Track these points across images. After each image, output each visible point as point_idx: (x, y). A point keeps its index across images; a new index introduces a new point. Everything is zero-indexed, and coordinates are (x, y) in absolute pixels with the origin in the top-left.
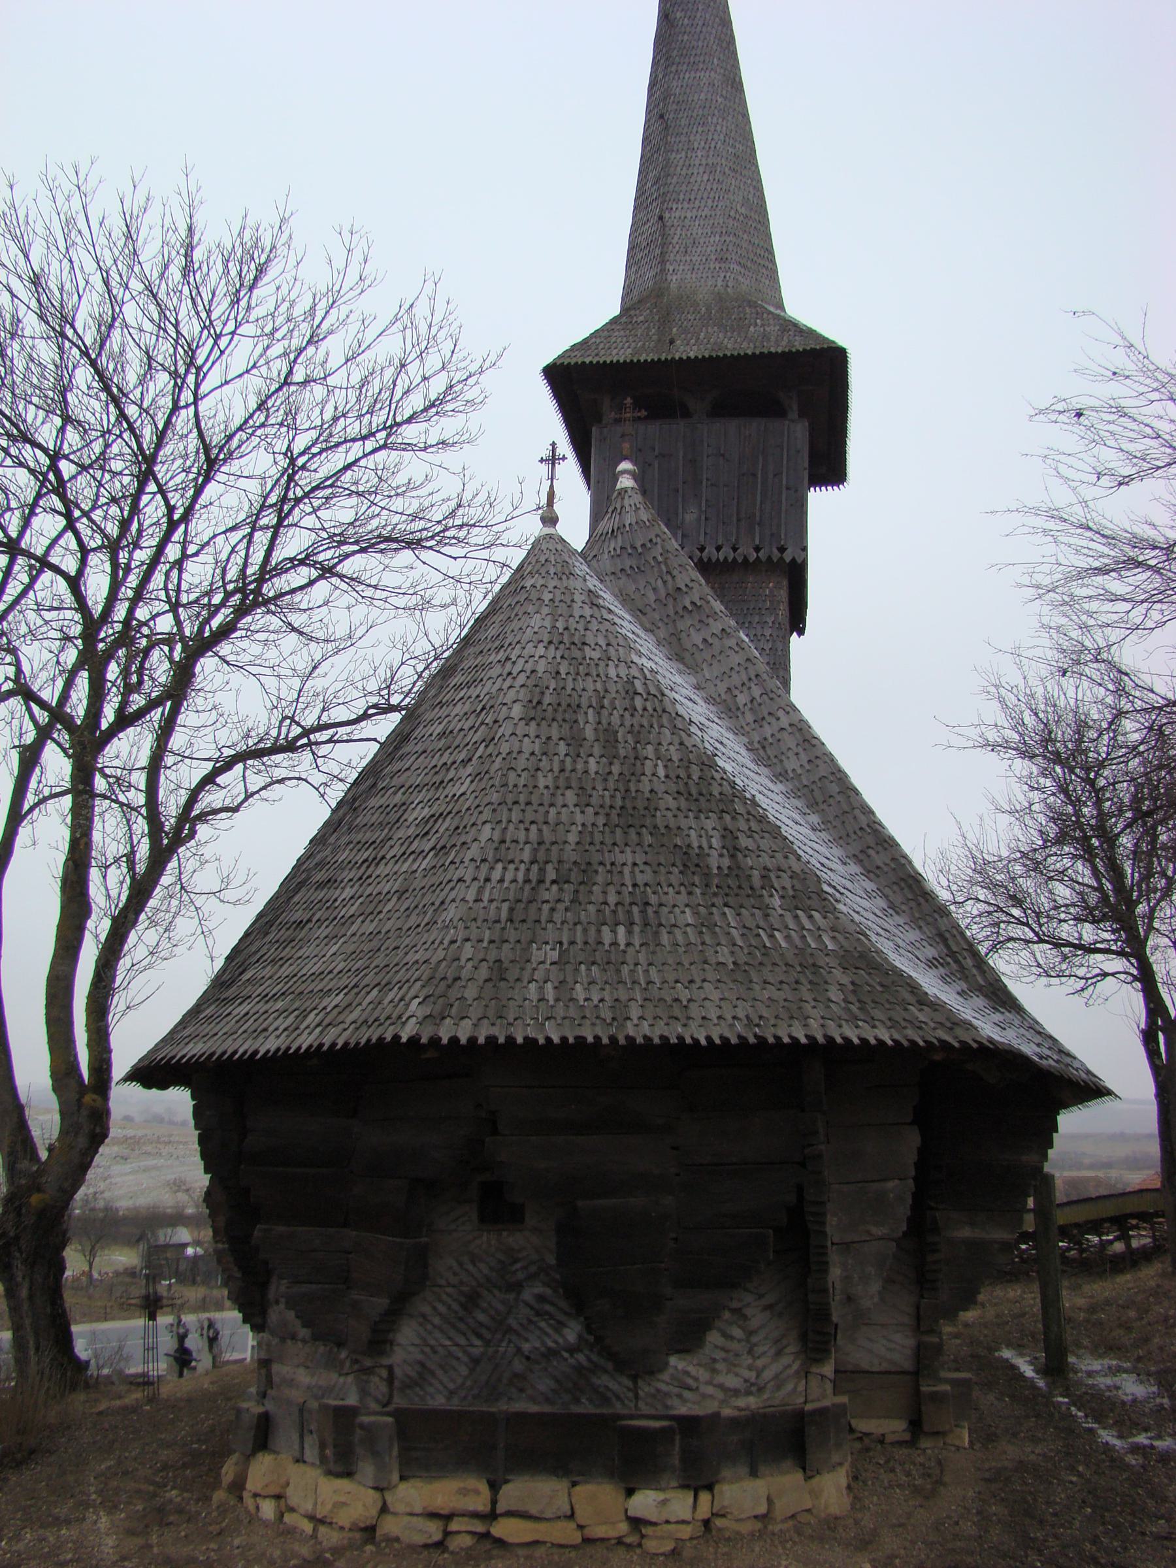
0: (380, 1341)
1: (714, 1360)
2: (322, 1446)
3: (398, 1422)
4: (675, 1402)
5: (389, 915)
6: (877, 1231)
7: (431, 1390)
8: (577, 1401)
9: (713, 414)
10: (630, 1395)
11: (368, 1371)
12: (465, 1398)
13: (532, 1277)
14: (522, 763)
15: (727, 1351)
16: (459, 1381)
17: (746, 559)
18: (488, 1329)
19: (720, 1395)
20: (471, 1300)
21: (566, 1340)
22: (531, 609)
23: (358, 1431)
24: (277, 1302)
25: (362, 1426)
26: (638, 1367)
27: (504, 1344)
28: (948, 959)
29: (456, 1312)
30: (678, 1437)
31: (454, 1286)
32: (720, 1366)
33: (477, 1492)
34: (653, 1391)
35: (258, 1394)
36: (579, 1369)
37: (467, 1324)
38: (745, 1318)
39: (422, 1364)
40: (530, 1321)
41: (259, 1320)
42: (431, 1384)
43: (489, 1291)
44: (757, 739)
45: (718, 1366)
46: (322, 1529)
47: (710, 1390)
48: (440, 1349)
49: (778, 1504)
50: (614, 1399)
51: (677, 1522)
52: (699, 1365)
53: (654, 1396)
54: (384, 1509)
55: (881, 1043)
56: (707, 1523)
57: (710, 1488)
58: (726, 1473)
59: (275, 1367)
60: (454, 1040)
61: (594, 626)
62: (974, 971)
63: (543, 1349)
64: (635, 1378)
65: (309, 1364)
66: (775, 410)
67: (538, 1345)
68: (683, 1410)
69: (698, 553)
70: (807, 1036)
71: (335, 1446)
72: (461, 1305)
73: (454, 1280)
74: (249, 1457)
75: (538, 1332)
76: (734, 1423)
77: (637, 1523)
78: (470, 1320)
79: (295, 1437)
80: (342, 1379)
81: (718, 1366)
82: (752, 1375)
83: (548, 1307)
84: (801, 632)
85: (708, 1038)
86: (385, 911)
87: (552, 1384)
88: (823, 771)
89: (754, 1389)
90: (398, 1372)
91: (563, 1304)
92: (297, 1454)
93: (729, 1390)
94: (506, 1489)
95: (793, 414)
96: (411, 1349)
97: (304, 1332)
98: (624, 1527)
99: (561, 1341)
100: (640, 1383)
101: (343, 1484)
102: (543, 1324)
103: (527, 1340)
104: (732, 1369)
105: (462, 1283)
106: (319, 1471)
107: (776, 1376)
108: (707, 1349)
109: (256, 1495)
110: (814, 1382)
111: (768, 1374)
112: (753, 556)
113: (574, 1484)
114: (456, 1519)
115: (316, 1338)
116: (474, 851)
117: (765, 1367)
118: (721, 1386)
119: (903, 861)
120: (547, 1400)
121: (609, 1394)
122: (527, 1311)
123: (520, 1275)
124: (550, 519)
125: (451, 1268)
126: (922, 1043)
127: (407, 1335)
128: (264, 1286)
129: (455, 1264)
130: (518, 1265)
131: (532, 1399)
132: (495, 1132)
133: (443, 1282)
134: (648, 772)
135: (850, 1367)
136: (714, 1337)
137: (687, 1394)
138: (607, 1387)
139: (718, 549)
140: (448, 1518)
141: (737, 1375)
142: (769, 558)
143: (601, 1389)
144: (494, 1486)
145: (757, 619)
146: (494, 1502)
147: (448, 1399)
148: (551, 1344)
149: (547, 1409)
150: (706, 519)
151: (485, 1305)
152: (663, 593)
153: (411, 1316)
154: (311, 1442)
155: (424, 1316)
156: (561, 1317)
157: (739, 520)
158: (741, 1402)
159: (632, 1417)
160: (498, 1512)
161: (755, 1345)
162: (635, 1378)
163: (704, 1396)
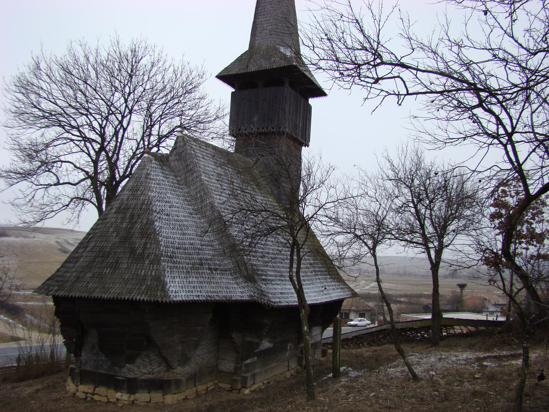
19: (141, 374)
38: (150, 357)
44: (200, 206)
47: (137, 372)
49: (152, 400)
56: (133, 402)
68: (129, 376)
76: (144, 380)
90: (82, 361)
94: (97, 389)
104: (142, 369)
107: (158, 371)
111: (155, 370)
118: (141, 372)
127: (83, 353)
139: (263, 129)
140: (87, 393)
152: (184, 166)
158: (147, 376)
162: (120, 368)
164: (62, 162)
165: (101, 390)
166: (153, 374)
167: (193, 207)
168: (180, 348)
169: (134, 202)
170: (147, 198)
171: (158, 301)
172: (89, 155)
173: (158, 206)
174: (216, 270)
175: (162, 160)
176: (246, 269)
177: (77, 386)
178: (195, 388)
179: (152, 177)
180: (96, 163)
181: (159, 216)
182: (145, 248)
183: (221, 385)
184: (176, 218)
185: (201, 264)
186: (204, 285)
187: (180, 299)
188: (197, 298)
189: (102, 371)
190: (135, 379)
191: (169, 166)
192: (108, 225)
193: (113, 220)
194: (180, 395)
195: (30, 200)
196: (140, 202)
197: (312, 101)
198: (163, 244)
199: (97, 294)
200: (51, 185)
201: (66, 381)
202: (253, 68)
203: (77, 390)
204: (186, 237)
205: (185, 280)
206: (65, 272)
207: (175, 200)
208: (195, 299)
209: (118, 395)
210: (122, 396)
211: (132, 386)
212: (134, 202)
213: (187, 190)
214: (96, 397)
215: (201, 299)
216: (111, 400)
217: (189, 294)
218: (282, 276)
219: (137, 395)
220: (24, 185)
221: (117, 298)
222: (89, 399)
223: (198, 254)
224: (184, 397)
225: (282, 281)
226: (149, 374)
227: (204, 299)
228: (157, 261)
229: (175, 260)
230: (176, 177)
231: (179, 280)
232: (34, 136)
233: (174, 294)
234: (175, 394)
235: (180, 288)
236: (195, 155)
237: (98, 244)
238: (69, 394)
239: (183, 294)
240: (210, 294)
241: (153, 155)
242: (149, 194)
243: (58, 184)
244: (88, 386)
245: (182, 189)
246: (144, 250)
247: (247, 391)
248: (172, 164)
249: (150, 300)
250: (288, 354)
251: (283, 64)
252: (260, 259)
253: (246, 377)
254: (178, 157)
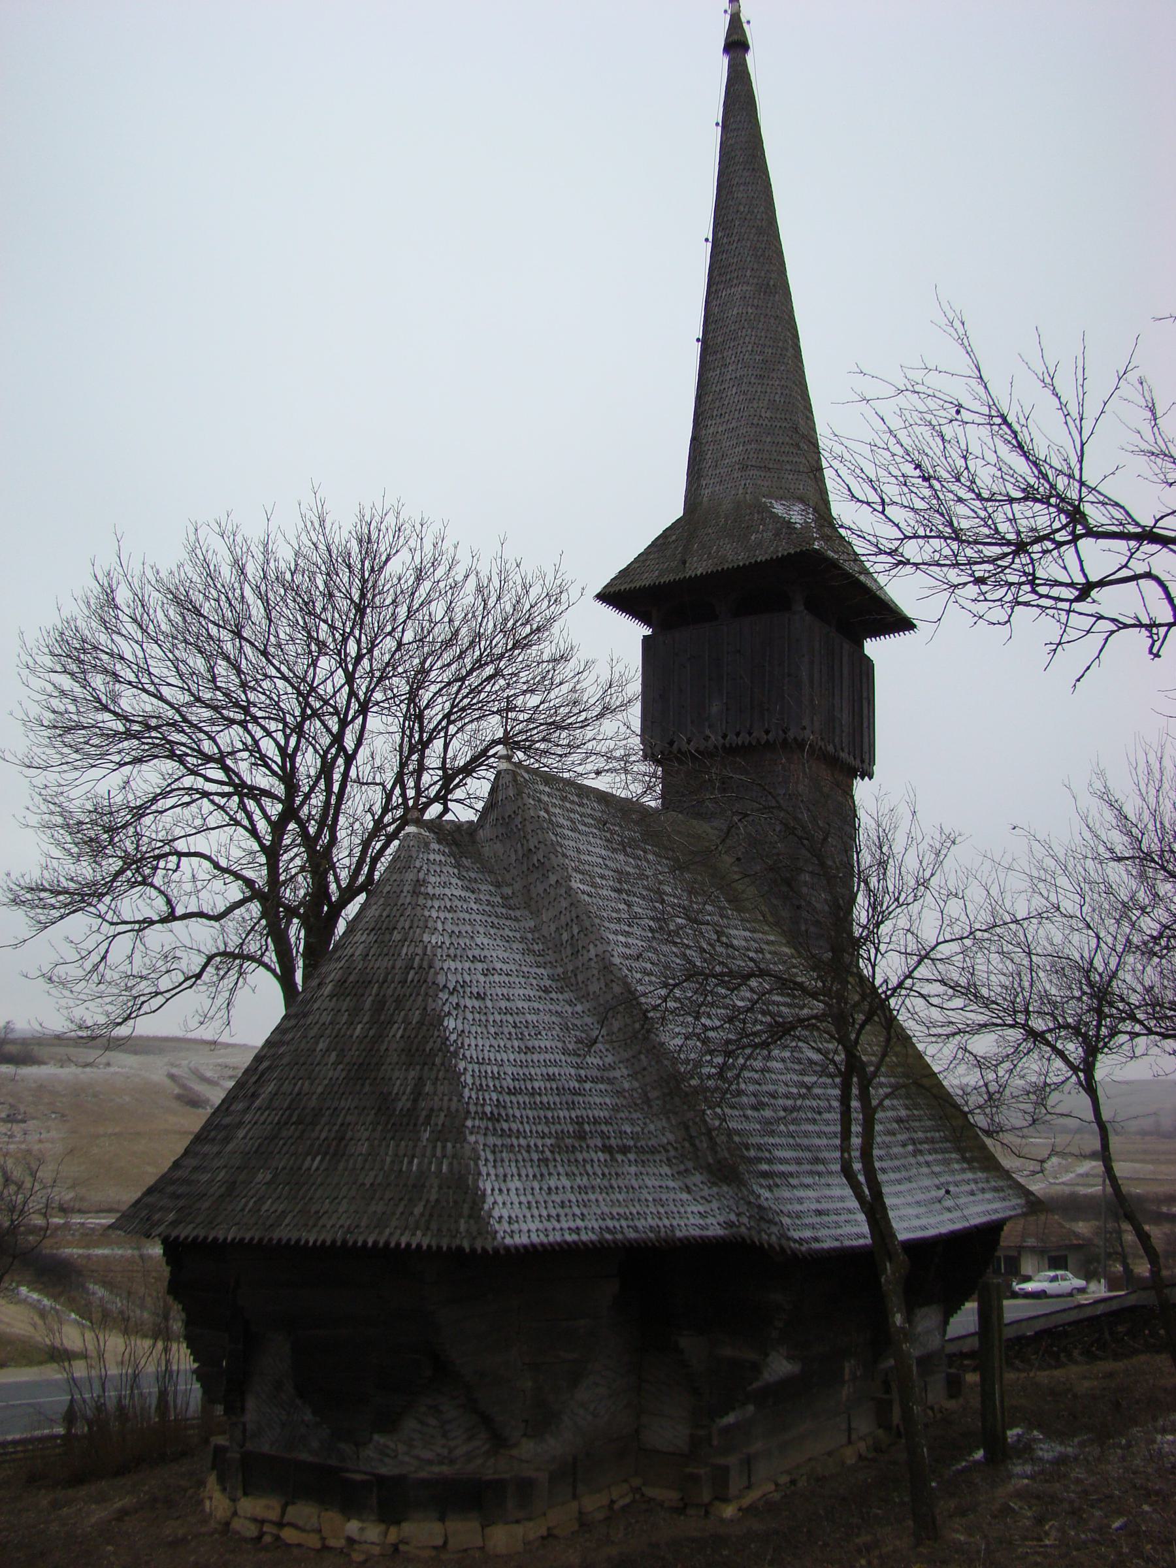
17: (758, 741)
44: (571, 968)
47: (407, 1459)
54: (235, 1514)
56: (396, 1548)
68: (383, 1471)
82: (445, 1452)
94: (291, 1510)
118: (417, 1458)
127: (251, 1403)
137: (386, 1460)
139: (738, 734)
140: (262, 1522)
152: (520, 853)
158: (436, 1469)
164: (180, 855)
165: (304, 1512)
166: (452, 1462)
167: (550, 971)
168: (530, 1384)
169: (385, 963)
170: (419, 951)
171: (460, 1249)
172: (254, 832)
173: (451, 971)
174: (625, 1150)
175: (458, 839)
176: (713, 1146)
177: (234, 1500)
178: (574, 1505)
179: (430, 890)
180: (272, 853)
181: (454, 1000)
182: (417, 1094)
183: (650, 1492)
184: (503, 1004)
185: (581, 1136)
186: (592, 1197)
187: (525, 1240)
188: (575, 1237)
189: (305, 1456)
190: (400, 1479)
191: (478, 857)
192: (312, 1033)
193: (326, 1018)
194: (531, 1524)
195: (96, 967)
196: (399, 964)
197: (873, 648)
198: (470, 1081)
199: (283, 1233)
200: (152, 923)
201: (202, 1483)
202: (699, 567)
203: (235, 1514)
204: (535, 1057)
205: (536, 1185)
206: (195, 1169)
207: (497, 953)
208: (568, 1238)
209: (353, 1527)
210: (362, 1529)
211: (391, 1500)
212: (385, 963)
213: (532, 924)
214: (289, 1535)
215: (584, 1237)
216: (332, 1542)
217: (549, 1226)
218: (817, 1161)
219: (407, 1528)
220: (79, 923)
221: (344, 1242)
222: (267, 1539)
223: (571, 1106)
224: (544, 1532)
225: (819, 1174)
226: (441, 1463)
227: (594, 1237)
228: (453, 1130)
229: (505, 1126)
230: (498, 885)
231: (519, 1184)
232: (102, 788)
233: (506, 1226)
234: (518, 1522)
235: (521, 1210)
236: (551, 821)
237: (286, 1087)
238: (213, 1524)
239: (533, 1227)
240: (610, 1223)
241: (436, 826)
242: (426, 938)
243: (170, 917)
244: (263, 1502)
245: (516, 919)
246: (415, 1101)
247: (729, 1511)
248: (487, 851)
249: (439, 1248)
250: (846, 1391)
251: (784, 548)
252: (749, 1112)
253: (726, 1469)
254: (502, 830)
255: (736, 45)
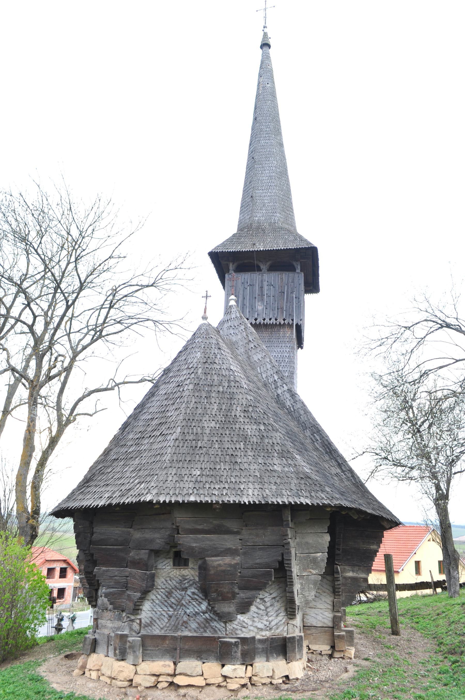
0: (136, 610)
1: (254, 617)
2: (115, 650)
3: (142, 640)
4: (239, 632)
5: (145, 458)
6: (314, 572)
7: (154, 628)
8: (205, 631)
9: (270, 267)
10: (224, 629)
11: (132, 621)
12: (166, 630)
13: (191, 585)
14: (191, 406)
15: (258, 614)
16: (164, 624)
18: (175, 604)
19: (256, 630)
20: (169, 594)
21: (202, 609)
22: (197, 350)
23: (128, 643)
24: (101, 596)
25: (129, 642)
26: (226, 618)
27: (180, 610)
28: (342, 474)
29: (164, 599)
30: (240, 645)
31: (164, 589)
32: (256, 619)
33: (169, 666)
34: (232, 628)
35: (93, 632)
36: (206, 619)
37: (167, 603)
39: (151, 618)
40: (190, 602)
41: (94, 603)
42: (154, 626)
43: (176, 591)
45: (255, 619)
46: (114, 681)
47: (252, 628)
48: (158, 612)
50: (218, 631)
51: (239, 678)
52: (248, 619)
53: (232, 630)
54: (136, 673)
55: (307, 504)
57: (252, 665)
58: (257, 660)
59: (100, 621)
60: (164, 501)
61: (219, 357)
62: (352, 478)
63: (194, 612)
64: (225, 623)
65: (112, 619)
66: (292, 269)
67: (192, 610)
68: (242, 636)
69: (263, 321)
70: (282, 501)
71: (120, 649)
72: (166, 596)
73: (164, 587)
74: (88, 655)
75: (192, 606)
76: (260, 641)
77: (225, 677)
78: (169, 602)
79: (106, 648)
80: (123, 624)
81: (255, 619)
83: (196, 597)
84: (302, 348)
85: (249, 502)
86: (144, 456)
87: (197, 625)
88: (299, 406)
89: (268, 628)
91: (201, 595)
92: (106, 654)
93: (259, 629)
94: (179, 665)
95: (298, 270)
96: (148, 612)
97: (110, 607)
98: (221, 679)
99: (200, 609)
100: (227, 624)
101: (122, 663)
102: (194, 603)
103: (188, 609)
104: (260, 620)
105: (166, 587)
106: (113, 659)
107: (277, 624)
108: (251, 613)
109: (90, 670)
110: (290, 627)
111: (273, 623)
112: (282, 322)
113: (204, 663)
114: (161, 676)
115: (114, 609)
116: (174, 437)
117: (272, 621)
118: (256, 627)
119: (326, 438)
120: (195, 631)
121: (216, 629)
122: (188, 598)
123: (187, 585)
124: (205, 318)
125: (163, 582)
126: (321, 504)
127: (146, 606)
128: (97, 590)
129: (164, 581)
130: (186, 581)
131: (190, 630)
132: (178, 533)
133: (160, 587)
134: (234, 409)
135: (309, 625)
136: (253, 608)
137: (244, 629)
138: (216, 627)
140: (158, 676)
141: (262, 623)
142: (289, 323)
143: (214, 627)
144: (175, 664)
145: (284, 345)
146: (175, 670)
147: (160, 631)
148: (197, 611)
149: (195, 634)
150: (266, 308)
151: (174, 596)
153: (148, 600)
154: (111, 648)
155: (153, 600)
156: (201, 601)
157: (278, 309)
159: (224, 638)
160: (176, 673)
161: (269, 612)
162: (225, 623)
163: (250, 630)
165: (189, 665)
211: (248, 651)
214: (179, 680)
255: (265, 45)
